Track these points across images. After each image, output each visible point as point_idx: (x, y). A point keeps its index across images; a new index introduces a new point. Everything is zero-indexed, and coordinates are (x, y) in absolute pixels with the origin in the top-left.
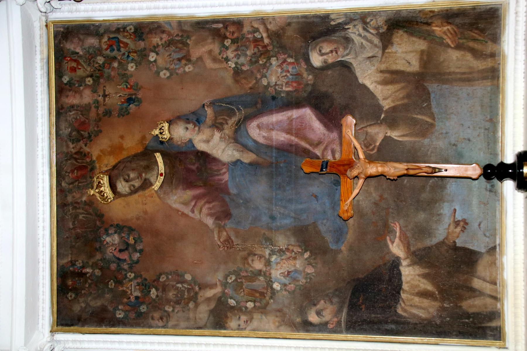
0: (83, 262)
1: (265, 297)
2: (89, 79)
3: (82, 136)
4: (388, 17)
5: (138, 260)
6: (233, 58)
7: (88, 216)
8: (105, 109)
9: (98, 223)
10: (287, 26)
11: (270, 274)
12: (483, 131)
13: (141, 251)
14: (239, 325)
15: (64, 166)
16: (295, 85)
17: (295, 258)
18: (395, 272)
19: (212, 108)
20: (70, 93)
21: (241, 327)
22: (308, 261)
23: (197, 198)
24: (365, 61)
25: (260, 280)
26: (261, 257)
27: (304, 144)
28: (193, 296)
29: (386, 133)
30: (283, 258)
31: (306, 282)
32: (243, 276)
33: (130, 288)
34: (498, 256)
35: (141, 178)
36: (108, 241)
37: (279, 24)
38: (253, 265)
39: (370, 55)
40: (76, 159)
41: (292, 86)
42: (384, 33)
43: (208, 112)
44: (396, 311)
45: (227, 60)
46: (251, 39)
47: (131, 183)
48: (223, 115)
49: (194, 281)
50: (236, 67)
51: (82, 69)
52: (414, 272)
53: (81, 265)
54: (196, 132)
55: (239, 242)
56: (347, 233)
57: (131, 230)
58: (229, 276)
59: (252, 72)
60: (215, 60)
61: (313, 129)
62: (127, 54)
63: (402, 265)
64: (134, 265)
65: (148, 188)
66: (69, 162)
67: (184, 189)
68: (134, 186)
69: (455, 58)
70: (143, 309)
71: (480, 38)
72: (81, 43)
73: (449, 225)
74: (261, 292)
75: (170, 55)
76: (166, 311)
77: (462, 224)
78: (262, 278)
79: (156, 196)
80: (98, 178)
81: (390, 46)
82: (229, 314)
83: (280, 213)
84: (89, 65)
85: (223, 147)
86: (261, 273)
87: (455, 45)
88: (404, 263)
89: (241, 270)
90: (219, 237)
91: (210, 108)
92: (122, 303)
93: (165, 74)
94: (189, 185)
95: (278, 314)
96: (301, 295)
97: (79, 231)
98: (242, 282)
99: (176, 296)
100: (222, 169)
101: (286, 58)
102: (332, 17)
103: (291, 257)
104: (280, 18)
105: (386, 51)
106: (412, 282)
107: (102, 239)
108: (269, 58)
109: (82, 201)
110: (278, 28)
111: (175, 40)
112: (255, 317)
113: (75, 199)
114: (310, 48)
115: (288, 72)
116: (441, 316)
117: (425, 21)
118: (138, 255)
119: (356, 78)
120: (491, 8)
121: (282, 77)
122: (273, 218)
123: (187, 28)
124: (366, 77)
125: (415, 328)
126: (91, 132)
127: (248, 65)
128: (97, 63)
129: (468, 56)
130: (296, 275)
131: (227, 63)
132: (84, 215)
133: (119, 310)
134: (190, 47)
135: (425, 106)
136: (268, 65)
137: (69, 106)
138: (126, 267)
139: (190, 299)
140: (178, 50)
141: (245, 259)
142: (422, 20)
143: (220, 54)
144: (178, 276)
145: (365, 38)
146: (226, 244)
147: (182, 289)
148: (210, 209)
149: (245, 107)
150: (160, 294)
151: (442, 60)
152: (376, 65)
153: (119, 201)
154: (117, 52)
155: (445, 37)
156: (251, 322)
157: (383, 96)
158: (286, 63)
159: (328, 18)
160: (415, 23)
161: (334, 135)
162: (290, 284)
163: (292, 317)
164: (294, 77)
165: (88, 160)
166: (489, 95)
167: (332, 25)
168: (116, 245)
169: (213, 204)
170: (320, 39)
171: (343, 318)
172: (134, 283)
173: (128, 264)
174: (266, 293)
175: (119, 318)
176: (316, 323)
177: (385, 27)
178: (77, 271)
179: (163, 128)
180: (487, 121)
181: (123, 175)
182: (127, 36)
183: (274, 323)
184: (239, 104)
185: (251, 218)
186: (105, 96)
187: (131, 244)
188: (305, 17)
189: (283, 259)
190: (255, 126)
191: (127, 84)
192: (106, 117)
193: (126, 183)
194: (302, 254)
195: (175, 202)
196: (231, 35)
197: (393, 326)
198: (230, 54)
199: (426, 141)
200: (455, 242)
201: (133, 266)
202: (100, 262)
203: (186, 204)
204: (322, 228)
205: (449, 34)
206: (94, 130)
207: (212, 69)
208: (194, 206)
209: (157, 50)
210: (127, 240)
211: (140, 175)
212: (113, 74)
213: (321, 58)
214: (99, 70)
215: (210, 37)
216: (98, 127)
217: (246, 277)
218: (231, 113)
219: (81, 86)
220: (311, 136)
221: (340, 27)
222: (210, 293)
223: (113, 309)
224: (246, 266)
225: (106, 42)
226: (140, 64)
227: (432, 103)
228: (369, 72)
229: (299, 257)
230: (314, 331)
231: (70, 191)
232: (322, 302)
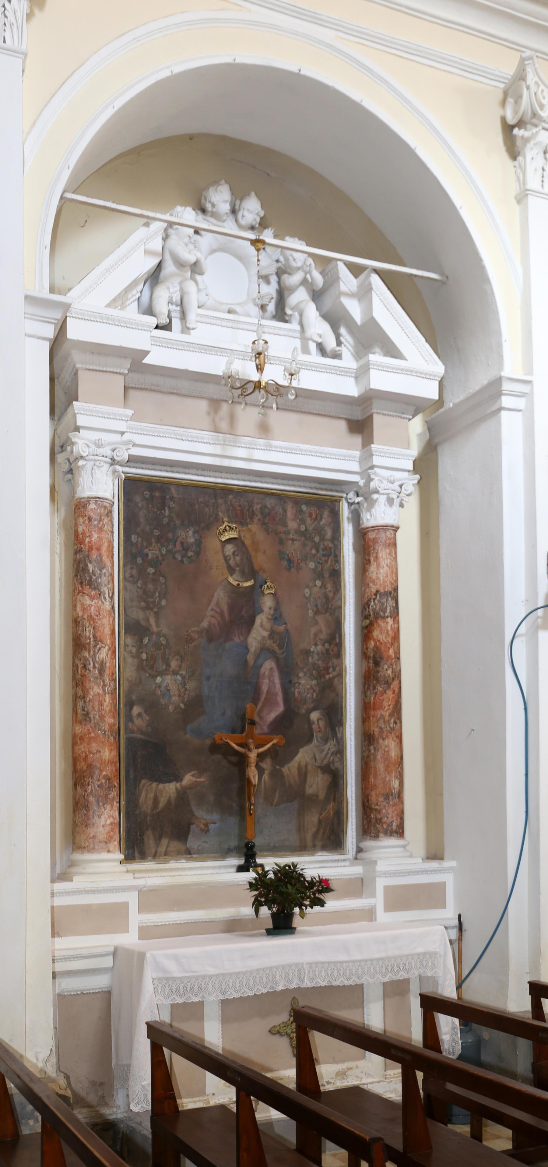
9: (203, 525)
11: (167, 674)
14: (128, 646)
16: (299, 698)
23: (222, 614)
26: (180, 667)
45: (316, 645)
47: (232, 558)
57: (198, 553)
60: (316, 635)
68: (230, 559)
70: (139, 560)
78: (164, 667)
90: (194, 632)
94: (232, 607)
102: (341, 728)
108: (316, 679)
115: (308, 693)
122: (208, 678)
138: (171, 547)
141: (178, 654)
145: (327, 753)
150: (151, 576)
168: (187, 539)
198: (320, 648)
203: (218, 604)
208: (216, 611)
211: (238, 566)
213: (315, 719)
218: (281, 647)
221: (334, 734)
222: (152, 621)
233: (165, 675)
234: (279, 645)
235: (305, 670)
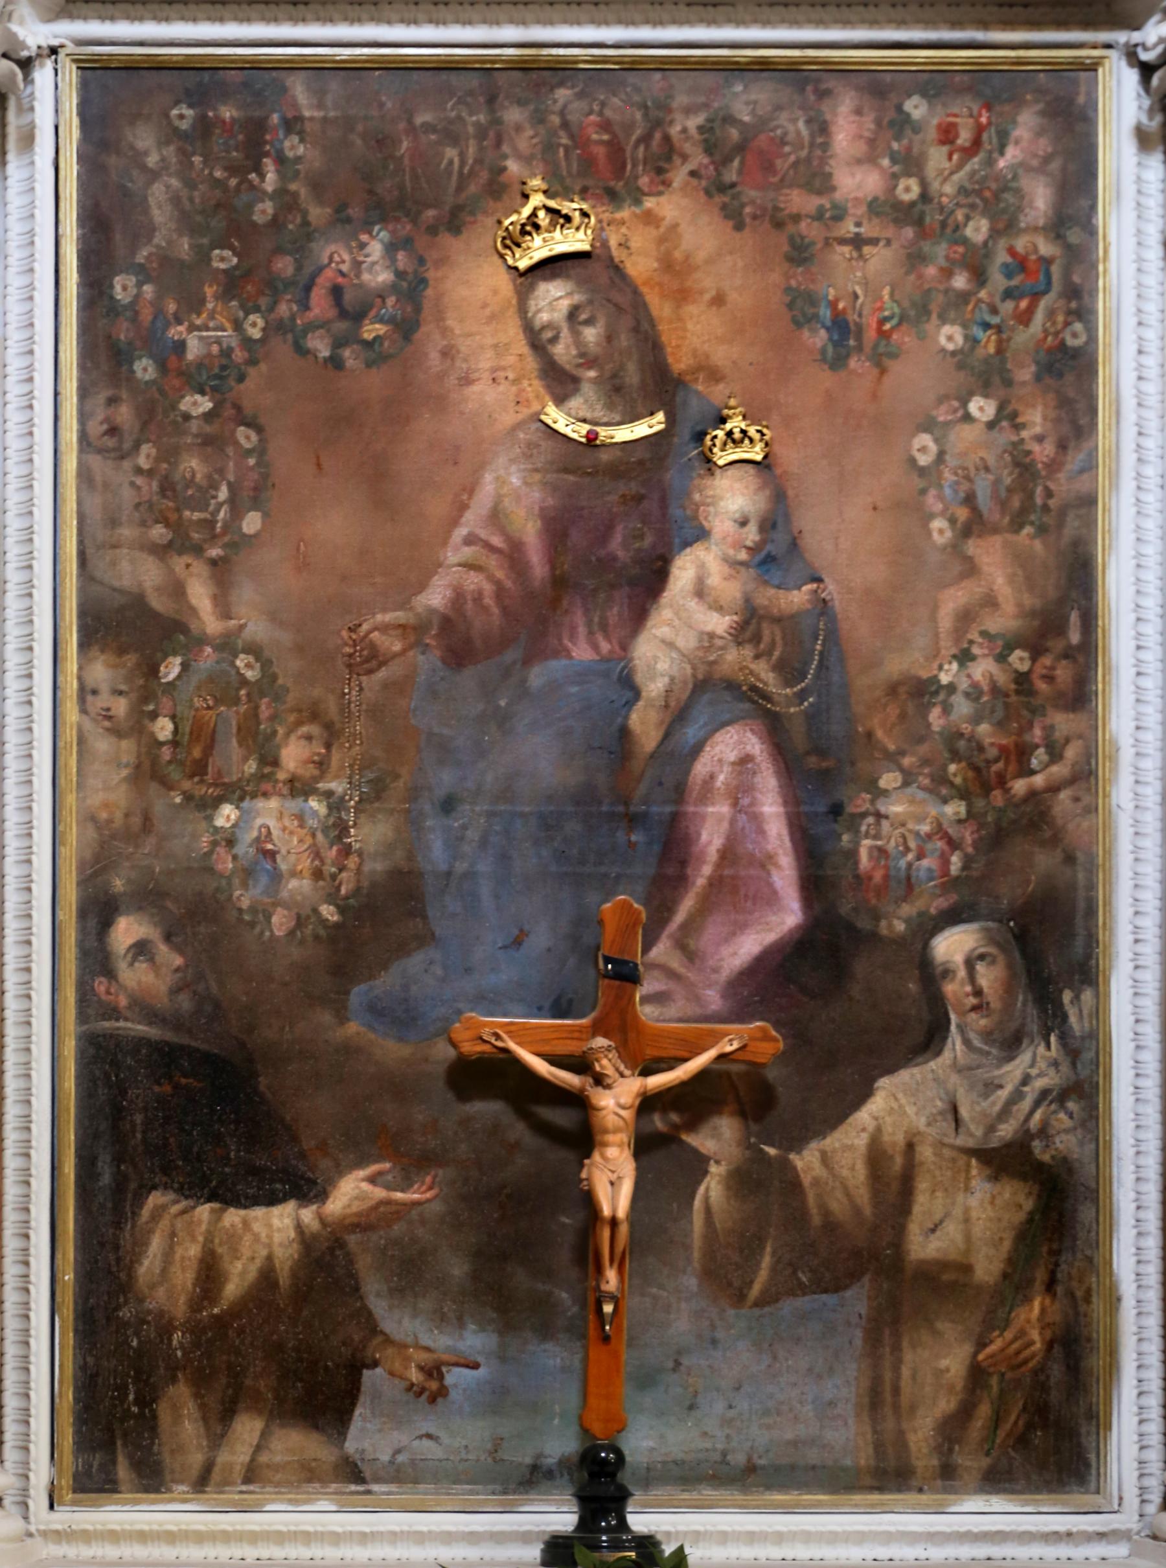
0: (298, 159)
1: (191, 776)
2: (916, 190)
3: (727, 160)
4: (1077, 1165)
6: (969, 676)
7: (455, 178)
8: (813, 243)
10: (1064, 851)
11: (265, 795)
12: (719, 1446)
13: (335, 362)
14: (95, 692)
15: (624, 97)
16: (878, 876)
17: (317, 874)
18: (278, 1186)
19: (809, 606)
20: (869, 123)
21: (90, 698)
22: (308, 917)
23: (514, 554)
24: (943, 1096)
25: (245, 759)
26: (322, 765)
27: (686, 906)
29: (717, 1162)
30: (320, 837)
31: (240, 910)
32: (257, 707)
33: (211, 324)
34: (334, 1487)
36: (368, 250)
37: (1071, 826)
38: (293, 738)
39: (964, 1112)
40: (646, 139)
41: (873, 868)
42: (1030, 1152)
43: (795, 592)
44: (154, 1187)
45: (965, 657)
46: (1027, 737)
47: (565, 333)
48: (785, 644)
49: (239, 543)
50: (941, 687)
51: (947, 165)
52: (281, 1245)
53: (290, 154)
54: (731, 552)
55: (367, 693)
56: (401, 1039)
58: (257, 659)
59: (921, 740)
60: (965, 617)
61: (734, 934)
62: (995, 320)
63: (300, 1206)
64: (290, 336)
65: (548, 388)
66: (638, 116)
68: (554, 340)
69: (944, 1363)
70: (144, 369)
71: (1001, 1434)
72: (1035, 163)
73: (428, 1349)
74: (206, 766)
75: (987, 469)
76: (137, 446)
77: (434, 1385)
78: (251, 767)
79: (520, 417)
80: (585, 214)
81: (988, 1172)
82: (131, 659)
83: (464, 827)
84: (962, 191)
85: (681, 643)
86: (267, 764)
87: (984, 1364)
88: (308, 1214)
89: (277, 698)
90: (384, 628)
91: (809, 601)
92: (160, 297)
93: (923, 450)
95: (136, 821)
96: (200, 893)
97: (405, 144)
98: (236, 701)
99: (190, 483)
100: (610, 642)
101: (962, 850)
102: (1087, 996)
104: (1093, 832)
105: (974, 1162)
106: (247, 1239)
107: (377, 228)
108: (964, 794)
109: (505, 157)
110: (1060, 822)
111: (1036, 485)
112: (125, 744)
113: (513, 133)
114: (990, 924)
115: (921, 856)
116: (144, 1322)
117: (1059, 1276)
118: (325, 353)
119: (890, 1070)
120: (1088, 1465)
121: (904, 837)
122: (448, 805)
123: (1072, 526)
124: (896, 1099)
125: (102, 1245)
126: (739, 193)
127: (944, 727)
128: (968, 218)
129: (948, 1401)
130: (264, 880)
131: (954, 657)
133: (140, 284)
134: (1009, 536)
135: (798, 1279)
136: (944, 791)
137: (828, 117)
139: (177, 527)
140: (1003, 494)
141: (314, 715)
142: (1064, 1267)
143: (984, 634)
144: (256, 489)
145: (1017, 1096)
146: (362, 650)
148: (478, 597)
149: (811, 717)
150: (194, 426)
151: (939, 1325)
152: (929, 1130)
153: (505, 285)
154: (1001, 289)
155: (1009, 1335)
156: (107, 730)
157: (834, 1151)
158: (946, 848)
159: (1083, 982)
160: (1055, 1246)
161: (714, 1000)
162: (235, 858)
163: (127, 864)
164: (903, 874)
166: (830, 1463)
167: (1061, 991)
168: (358, 276)
169: (496, 610)
170: (1017, 955)
171: (129, 1025)
172: (228, 335)
173: (293, 318)
174: (202, 781)
175: (112, 287)
177: (1046, 1158)
178: (268, 137)
179: (747, 441)
180: (749, 1459)
181: (590, 302)
182: (1054, 323)
183: (106, 805)
184: (819, 696)
185: (446, 731)
186: (858, 242)
187: (361, 327)
188: (1091, 911)
189: (314, 835)
190: (749, 748)
191: (894, 322)
192: (786, 248)
194: (332, 897)
195: (500, 481)
196: (1044, 671)
197: (106, 1179)
198: (983, 669)
199: (691, 1282)
200: (375, 1364)
201: (284, 334)
202: (298, 220)
203: (496, 517)
204: (415, 962)
205: (1016, 1346)
206: (743, 206)
207: (935, 608)
208: (488, 546)
209: (1004, 424)
210: (372, 313)
212: (931, 271)
213: (959, 959)
214: (944, 225)
215: (1038, 603)
216: (755, 217)
217: (256, 716)
218: (789, 671)
219: (894, 161)
220: (713, 929)
222: (200, 595)
223: (141, 265)
224: (292, 718)
225: (1036, 249)
226: (960, 366)
227: (807, 1298)
228: (910, 1110)
229: (323, 888)
230: (82, 931)
231: (539, 119)
232: (178, 961)
233: (254, 796)
234: (780, 667)
235: (907, 761)
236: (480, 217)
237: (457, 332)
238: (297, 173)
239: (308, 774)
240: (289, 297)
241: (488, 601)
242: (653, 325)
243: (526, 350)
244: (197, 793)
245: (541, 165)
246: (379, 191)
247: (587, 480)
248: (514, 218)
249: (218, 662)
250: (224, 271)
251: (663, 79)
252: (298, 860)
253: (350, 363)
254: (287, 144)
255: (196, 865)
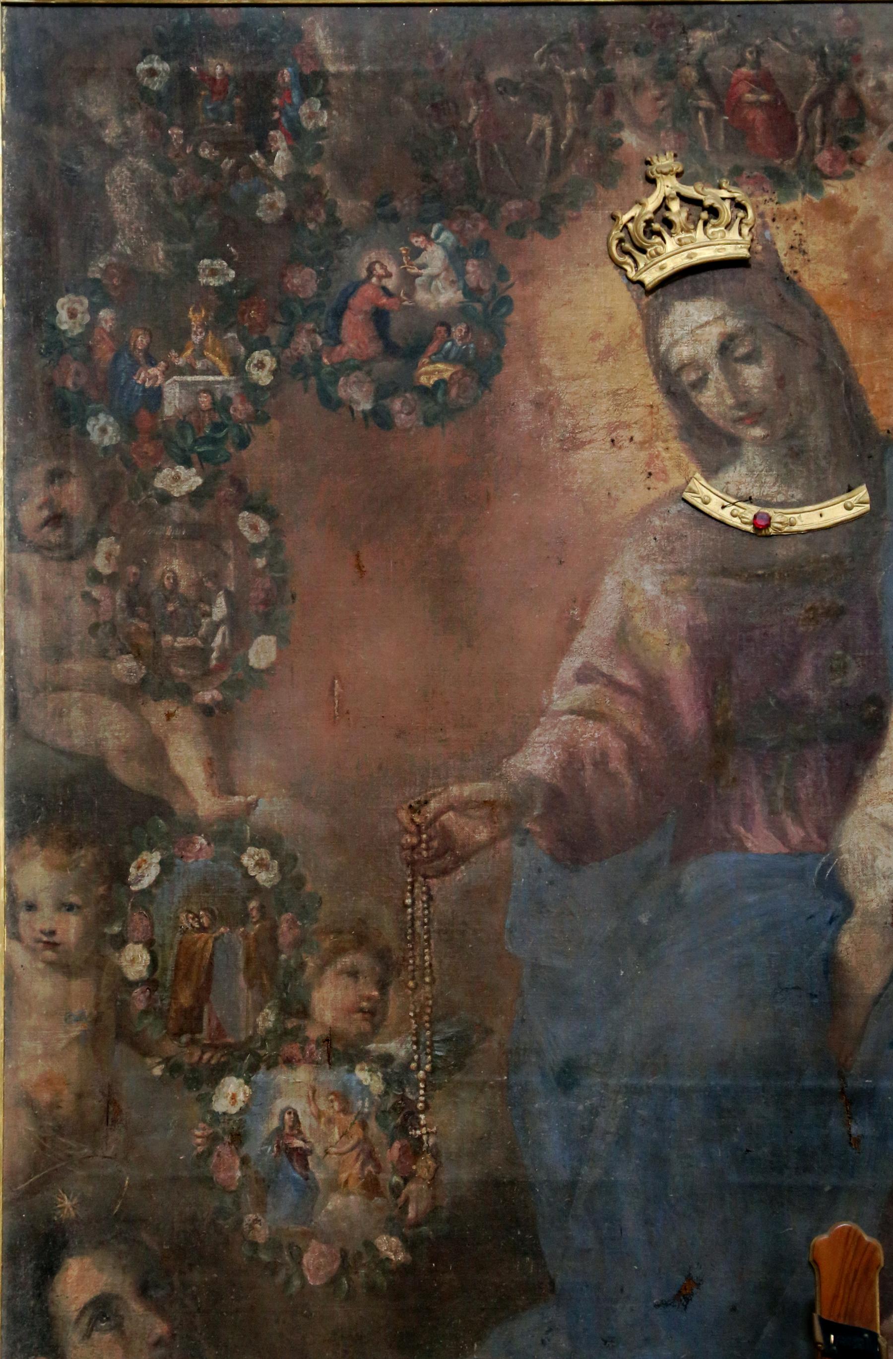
0: (321, 132)
1: (177, 1035)
5: (340, 403)
11: (289, 1062)
14: (31, 907)
15: (789, 41)
17: (371, 1187)
21: (23, 916)
28: (170, 674)
30: (373, 1124)
31: (254, 1245)
32: (275, 927)
33: (199, 365)
35: (741, 420)
38: (329, 972)
40: (824, 99)
47: (715, 373)
53: (309, 125)
58: (274, 855)
64: (313, 381)
65: (693, 452)
66: (812, 67)
67: (694, 635)
68: (700, 383)
74: (200, 1018)
76: (93, 541)
78: (268, 1019)
80: (738, 206)
82: (86, 856)
86: (291, 1015)
89: (304, 913)
95: (95, 1103)
96: (193, 1219)
98: (244, 918)
99: (172, 593)
103: (378, 1167)
112: (77, 985)
113: (630, 94)
118: (367, 406)
130: (290, 1196)
132: (549, 140)
133: (94, 310)
138: (303, 343)
144: (266, 603)
147: (205, 621)
150: (175, 512)
156: (50, 964)
162: (245, 1161)
163: (80, 1173)
165: (823, 158)
168: (410, 295)
169: (628, 779)
173: (317, 357)
174: (193, 1042)
175: (54, 312)
176: (51, 1295)
178: (276, 101)
181: (751, 330)
183: (48, 1081)
187: (416, 367)
189: (364, 1126)
193: (714, 343)
201: (306, 377)
208: (612, 683)
210: (433, 348)
211: (755, 416)
217: (274, 940)
223: (96, 281)
224: (327, 943)
229: (380, 1209)
236: (585, 211)
237: (557, 374)
238: (319, 151)
239: (353, 1030)
240: (311, 326)
241: (616, 765)
242: (846, 363)
243: (658, 398)
244: (186, 1060)
245: (672, 136)
246: (438, 176)
247: (756, 585)
248: (635, 211)
249: (214, 860)
250: (218, 290)
251: (847, 14)
252: (340, 1164)
253: (401, 419)
254: (304, 110)
255: (185, 1174)
